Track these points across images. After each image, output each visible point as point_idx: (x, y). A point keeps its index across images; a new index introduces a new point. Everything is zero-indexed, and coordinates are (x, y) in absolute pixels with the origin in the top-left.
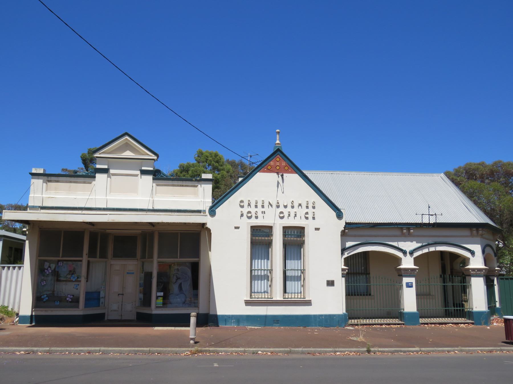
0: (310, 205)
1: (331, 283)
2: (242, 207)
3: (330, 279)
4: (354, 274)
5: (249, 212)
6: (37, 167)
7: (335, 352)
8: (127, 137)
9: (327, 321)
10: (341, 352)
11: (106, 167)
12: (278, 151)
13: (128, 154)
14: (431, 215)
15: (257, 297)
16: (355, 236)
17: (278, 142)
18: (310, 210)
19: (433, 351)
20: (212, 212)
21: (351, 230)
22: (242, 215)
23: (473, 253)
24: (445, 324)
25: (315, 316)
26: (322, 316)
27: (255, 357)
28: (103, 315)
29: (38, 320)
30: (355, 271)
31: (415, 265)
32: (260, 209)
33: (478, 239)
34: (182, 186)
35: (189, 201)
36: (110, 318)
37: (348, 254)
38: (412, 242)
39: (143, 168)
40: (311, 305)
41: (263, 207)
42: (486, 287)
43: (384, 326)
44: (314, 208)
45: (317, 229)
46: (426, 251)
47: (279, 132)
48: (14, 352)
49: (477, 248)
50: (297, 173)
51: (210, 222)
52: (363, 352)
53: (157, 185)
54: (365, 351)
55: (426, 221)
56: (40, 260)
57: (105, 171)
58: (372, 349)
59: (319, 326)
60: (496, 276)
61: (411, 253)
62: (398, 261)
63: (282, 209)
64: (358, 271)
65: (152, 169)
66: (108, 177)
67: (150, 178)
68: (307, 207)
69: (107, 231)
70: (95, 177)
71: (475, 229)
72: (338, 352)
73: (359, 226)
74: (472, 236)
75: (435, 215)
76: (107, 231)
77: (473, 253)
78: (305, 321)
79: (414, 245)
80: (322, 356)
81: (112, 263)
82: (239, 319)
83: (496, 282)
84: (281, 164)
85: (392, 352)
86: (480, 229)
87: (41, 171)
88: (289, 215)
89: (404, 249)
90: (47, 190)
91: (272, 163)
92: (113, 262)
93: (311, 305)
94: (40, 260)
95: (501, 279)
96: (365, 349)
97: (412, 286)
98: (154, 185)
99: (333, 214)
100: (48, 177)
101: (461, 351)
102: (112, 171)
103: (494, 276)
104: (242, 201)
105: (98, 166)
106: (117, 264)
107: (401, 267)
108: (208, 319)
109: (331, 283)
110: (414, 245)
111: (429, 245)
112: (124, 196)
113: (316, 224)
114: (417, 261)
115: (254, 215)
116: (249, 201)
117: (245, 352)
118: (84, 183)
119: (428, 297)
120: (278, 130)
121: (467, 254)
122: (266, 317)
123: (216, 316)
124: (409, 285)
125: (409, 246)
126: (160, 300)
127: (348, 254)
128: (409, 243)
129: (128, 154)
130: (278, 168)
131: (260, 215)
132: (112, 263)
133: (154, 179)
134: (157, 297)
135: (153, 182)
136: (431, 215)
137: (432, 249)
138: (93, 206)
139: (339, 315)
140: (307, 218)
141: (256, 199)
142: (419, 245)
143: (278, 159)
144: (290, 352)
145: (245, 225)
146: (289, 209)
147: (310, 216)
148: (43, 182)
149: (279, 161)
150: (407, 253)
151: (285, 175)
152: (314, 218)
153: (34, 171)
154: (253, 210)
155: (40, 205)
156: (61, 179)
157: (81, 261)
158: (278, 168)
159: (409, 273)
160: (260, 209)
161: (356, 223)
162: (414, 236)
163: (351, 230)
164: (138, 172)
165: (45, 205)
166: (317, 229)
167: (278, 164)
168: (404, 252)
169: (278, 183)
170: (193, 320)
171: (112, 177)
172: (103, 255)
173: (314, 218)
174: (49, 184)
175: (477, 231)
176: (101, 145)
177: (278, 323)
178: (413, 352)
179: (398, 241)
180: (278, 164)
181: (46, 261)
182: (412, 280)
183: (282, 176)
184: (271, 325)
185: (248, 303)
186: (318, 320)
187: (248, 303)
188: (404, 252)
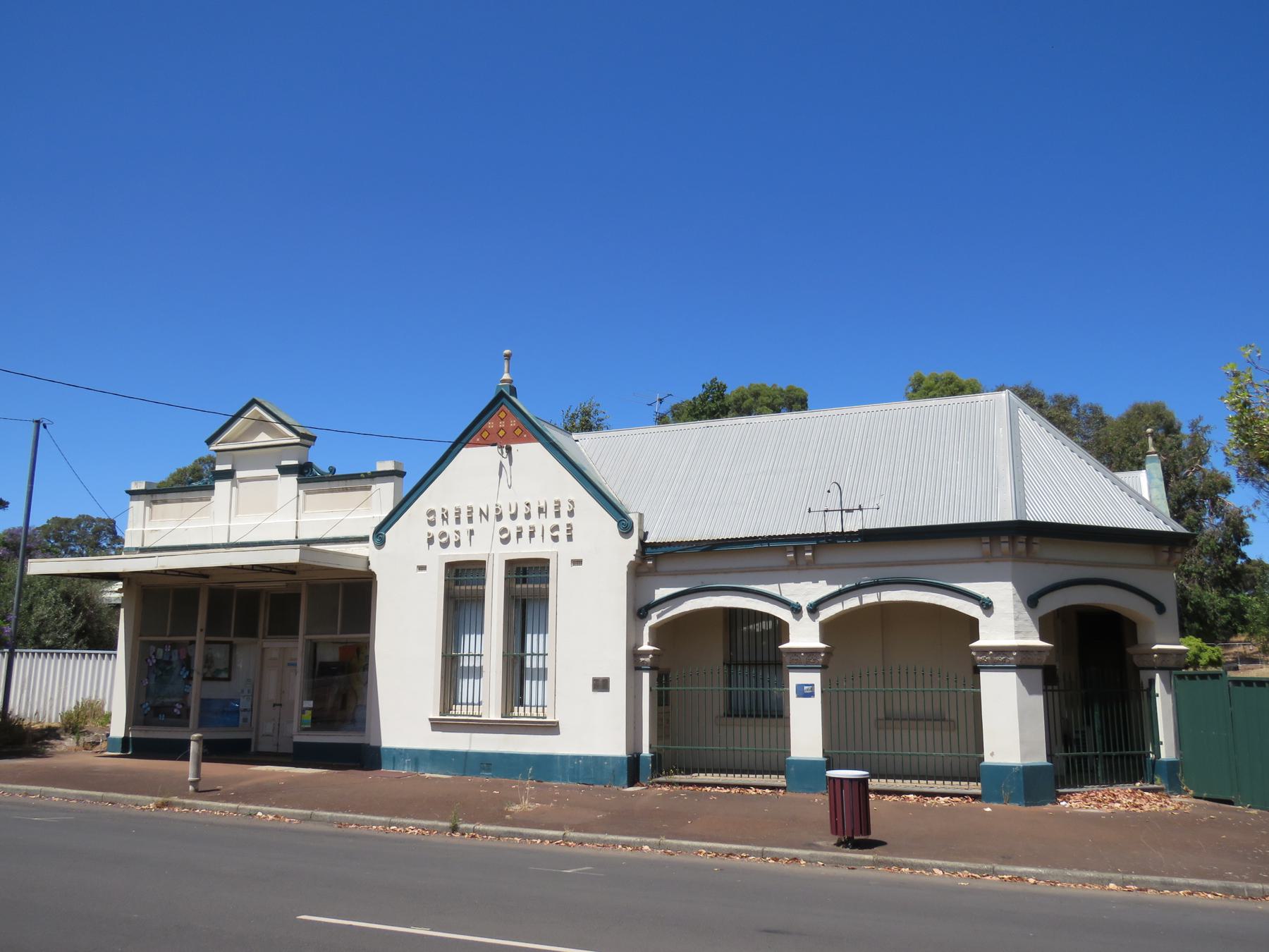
0: (564, 509)
1: (601, 685)
2: (432, 523)
3: (601, 675)
4: (750, 664)
5: (443, 534)
6: (382, 459)
7: (1103, 882)
8: (256, 408)
9: (586, 770)
10: (398, 825)
11: (229, 467)
12: (501, 399)
13: (263, 438)
14: (848, 511)
15: (460, 712)
16: (675, 574)
17: (506, 376)
18: (564, 520)
19: (592, 841)
20: (379, 536)
21: (652, 559)
22: (431, 541)
23: (987, 606)
24: (933, 795)
25: (564, 758)
26: (578, 757)
27: (1018, 886)
28: (247, 743)
29: (132, 747)
30: (766, 658)
31: (1042, 639)
32: (464, 527)
33: (1008, 566)
34: (346, 490)
35: (334, 521)
36: (262, 748)
37: (658, 616)
38: (815, 581)
39: (284, 463)
40: (558, 733)
41: (470, 520)
42: (1038, 701)
43: (752, 791)
44: (571, 514)
45: (577, 562)
46: (852, 603)
47: (508, 357)
48: (252, 814)
49: (1003, 593)
50: (538, 440)
51: (380, 562)
52: (441, 831)
53: (307, 493)
54: (446, 829)
55: (834, 525)
56: (143, 642)
57: (228, 475)
58: (463, 826)
59: (573, 780)
60: (1160, 669)
61: (814, 609)
62: (780, 630)
63: (506, 522)
64: (759, 658)
65: (296, 462)
66: (232, 485)
67: (292, 480)
68: (558, 514)
69: (237, 585)
70: (212, 488)
71: (1023, 539)
72: (905, 865)
73: (672, 549)
74: (987, 558)
75: (860, 509)
76: (237, 585)
77: (987, 606)
78: (543, 766)
79: (823, 588)
80: (362, 830)
81: (266, 645)
82: (419, 758)
83: (1159, 686)
84: (507, 423)
85: (499, 836)
86: (1036, 540)
87: (142, 487)
88: (519, 535)
89: (793, 600)
90: (151, 518)
91: (490, 425)
92: (267, 644)
93: (558, 733)
94: (143, 642)
95: (1181, 677)
96: (447, 824)
97: (811, 695)
98: (301, 492)
99: (611, 524)
100: (154, 493)
101: (659, 846)
102: (239, 474)
103: (1153, 669)
104: (431, 513)
105: (218, 468)
106: (274, 646)
107: (982, 642)
108: (366, 757)
109: (601, 685)
110: (823, 588)
111: (858, 588)
112: (254, 521)
113: (573, 550)
114: (827, 630)
115: (514, 536)
116: (572, 502)
117: (237, 811)
118: (182, 501)
119: (938, 724)
120: (507, 352)
121: (973, 610)
122: (466, 755)
123: (378, 749)
124: (805, 692)
125: (805, 592)
126: (308, 716)
127: (658, 616)
128: (807, 586)
129: (263, 438)
130: (502, 433)
131: (464, 538)
132: (266, 645)
133: (300, 482)
134: (303, 711)
135: (299, 488)
136: (848, 511)
137: (870, 598)
138: (209, 542)
139: (615, 759)
140: (555, 539)
141: (457, 505)
142: (835, 588)
143: (502, 415)
144: (309, 818)
145: (437, 559)
146: (521, 521)
147: (562, 534)
148: (146, 505)
149: (498, 420)
150: (802, 611)
151: (514, 447)
152: (570, 538)
153: (133, 488)
154: (450, 528)
155: (139, 545)
156: (170, 496)
157: (193, 642)
158: (502, 433)
159: (805, 659)
160: (464, 527)
161: (669, 544)
162: (822, 567)
163: (652, 559)
164: (275, 472)
165: (147, 545)
166: (577, 562)
167: (502, 424)
168: (796, 610)
169: (501, 465)
170: (193, 747)
171: (241, 485)
172: (252, 633)
173: (570, 538)
174: (155, 507)
175: (1028, 543)
176: (213, 432)
177: (489, 770)
178: (543, 838)
179: (779, 581)
180: (502, 424)
181: (151, 643)
182: (814, 678)
183: (509, 450)
184: (477, 773)
185: (436, 725)
186: (569, 766)
187: (436, 725)
188: (796, 610)
